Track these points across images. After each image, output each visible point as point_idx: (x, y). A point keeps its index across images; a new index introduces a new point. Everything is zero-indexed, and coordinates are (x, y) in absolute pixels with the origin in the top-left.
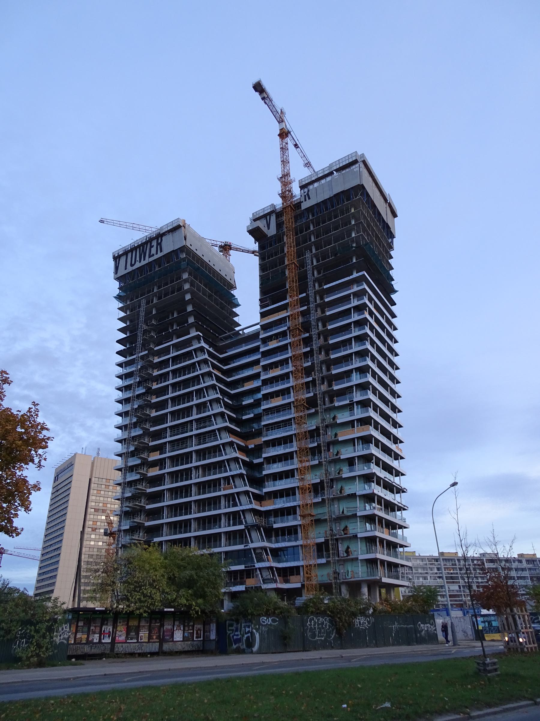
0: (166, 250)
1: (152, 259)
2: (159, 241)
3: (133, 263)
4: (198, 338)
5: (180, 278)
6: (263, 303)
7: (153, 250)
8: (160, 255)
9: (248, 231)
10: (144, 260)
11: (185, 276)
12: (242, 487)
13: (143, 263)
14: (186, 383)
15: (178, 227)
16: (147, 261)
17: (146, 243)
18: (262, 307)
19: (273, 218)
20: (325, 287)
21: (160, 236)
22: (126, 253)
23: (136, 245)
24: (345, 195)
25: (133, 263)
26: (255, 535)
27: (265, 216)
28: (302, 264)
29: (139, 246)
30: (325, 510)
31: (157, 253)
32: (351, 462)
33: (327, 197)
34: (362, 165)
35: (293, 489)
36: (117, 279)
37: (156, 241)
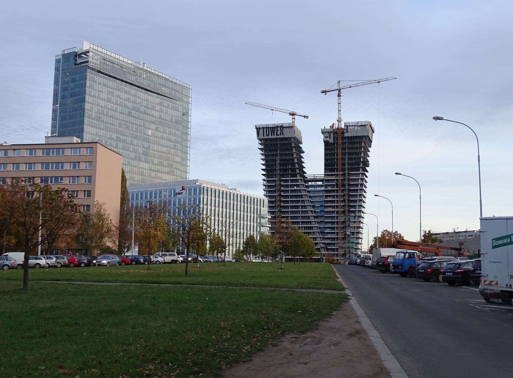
0: (286, 136)
1: (278, 137)
2: (282, 129)
3: (268, 135)
4: (301, 179)
5: (292, 150)
6: (326, 170)
7: (279, 133)
8: (282, 136)
9: (324, 141)
10: (274, 135)
11: (294, 151)
12: (317, 236)
13: (273, 137)
14: (296, 196)
15: (293, 127)
16: (275, 137)
17: (275, 127)
18: (325, 172)
19: (332, 134)
20: (351, 173)
21: (282, 127)
22: (263, 128)
23: (269, 127)
24: (362, 137)
25: (268, 135)
26: (323, 250)
27: (329, 132)
28: (343, 159)
29: (271, 127)
30: (344, 245)
31: (281, 135)
32: (353, 233)
33: (355, 135)
34: (369, 126)
35: (334, 238)
36: (260, 140)
37: (280, 128)
